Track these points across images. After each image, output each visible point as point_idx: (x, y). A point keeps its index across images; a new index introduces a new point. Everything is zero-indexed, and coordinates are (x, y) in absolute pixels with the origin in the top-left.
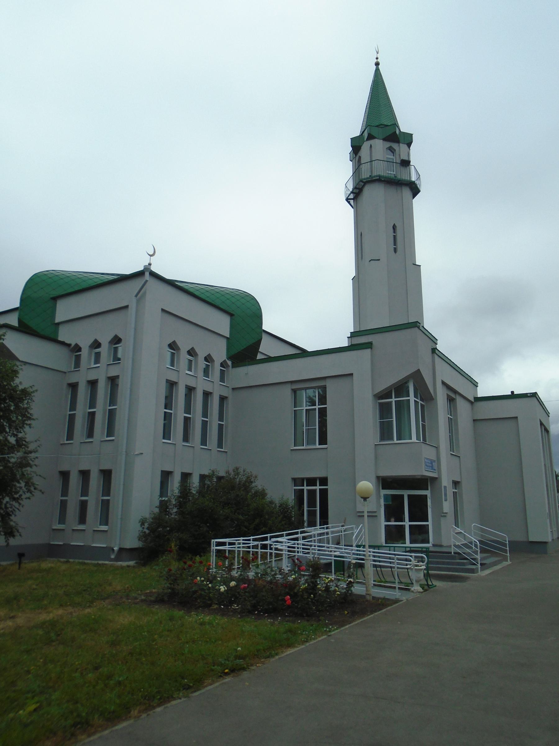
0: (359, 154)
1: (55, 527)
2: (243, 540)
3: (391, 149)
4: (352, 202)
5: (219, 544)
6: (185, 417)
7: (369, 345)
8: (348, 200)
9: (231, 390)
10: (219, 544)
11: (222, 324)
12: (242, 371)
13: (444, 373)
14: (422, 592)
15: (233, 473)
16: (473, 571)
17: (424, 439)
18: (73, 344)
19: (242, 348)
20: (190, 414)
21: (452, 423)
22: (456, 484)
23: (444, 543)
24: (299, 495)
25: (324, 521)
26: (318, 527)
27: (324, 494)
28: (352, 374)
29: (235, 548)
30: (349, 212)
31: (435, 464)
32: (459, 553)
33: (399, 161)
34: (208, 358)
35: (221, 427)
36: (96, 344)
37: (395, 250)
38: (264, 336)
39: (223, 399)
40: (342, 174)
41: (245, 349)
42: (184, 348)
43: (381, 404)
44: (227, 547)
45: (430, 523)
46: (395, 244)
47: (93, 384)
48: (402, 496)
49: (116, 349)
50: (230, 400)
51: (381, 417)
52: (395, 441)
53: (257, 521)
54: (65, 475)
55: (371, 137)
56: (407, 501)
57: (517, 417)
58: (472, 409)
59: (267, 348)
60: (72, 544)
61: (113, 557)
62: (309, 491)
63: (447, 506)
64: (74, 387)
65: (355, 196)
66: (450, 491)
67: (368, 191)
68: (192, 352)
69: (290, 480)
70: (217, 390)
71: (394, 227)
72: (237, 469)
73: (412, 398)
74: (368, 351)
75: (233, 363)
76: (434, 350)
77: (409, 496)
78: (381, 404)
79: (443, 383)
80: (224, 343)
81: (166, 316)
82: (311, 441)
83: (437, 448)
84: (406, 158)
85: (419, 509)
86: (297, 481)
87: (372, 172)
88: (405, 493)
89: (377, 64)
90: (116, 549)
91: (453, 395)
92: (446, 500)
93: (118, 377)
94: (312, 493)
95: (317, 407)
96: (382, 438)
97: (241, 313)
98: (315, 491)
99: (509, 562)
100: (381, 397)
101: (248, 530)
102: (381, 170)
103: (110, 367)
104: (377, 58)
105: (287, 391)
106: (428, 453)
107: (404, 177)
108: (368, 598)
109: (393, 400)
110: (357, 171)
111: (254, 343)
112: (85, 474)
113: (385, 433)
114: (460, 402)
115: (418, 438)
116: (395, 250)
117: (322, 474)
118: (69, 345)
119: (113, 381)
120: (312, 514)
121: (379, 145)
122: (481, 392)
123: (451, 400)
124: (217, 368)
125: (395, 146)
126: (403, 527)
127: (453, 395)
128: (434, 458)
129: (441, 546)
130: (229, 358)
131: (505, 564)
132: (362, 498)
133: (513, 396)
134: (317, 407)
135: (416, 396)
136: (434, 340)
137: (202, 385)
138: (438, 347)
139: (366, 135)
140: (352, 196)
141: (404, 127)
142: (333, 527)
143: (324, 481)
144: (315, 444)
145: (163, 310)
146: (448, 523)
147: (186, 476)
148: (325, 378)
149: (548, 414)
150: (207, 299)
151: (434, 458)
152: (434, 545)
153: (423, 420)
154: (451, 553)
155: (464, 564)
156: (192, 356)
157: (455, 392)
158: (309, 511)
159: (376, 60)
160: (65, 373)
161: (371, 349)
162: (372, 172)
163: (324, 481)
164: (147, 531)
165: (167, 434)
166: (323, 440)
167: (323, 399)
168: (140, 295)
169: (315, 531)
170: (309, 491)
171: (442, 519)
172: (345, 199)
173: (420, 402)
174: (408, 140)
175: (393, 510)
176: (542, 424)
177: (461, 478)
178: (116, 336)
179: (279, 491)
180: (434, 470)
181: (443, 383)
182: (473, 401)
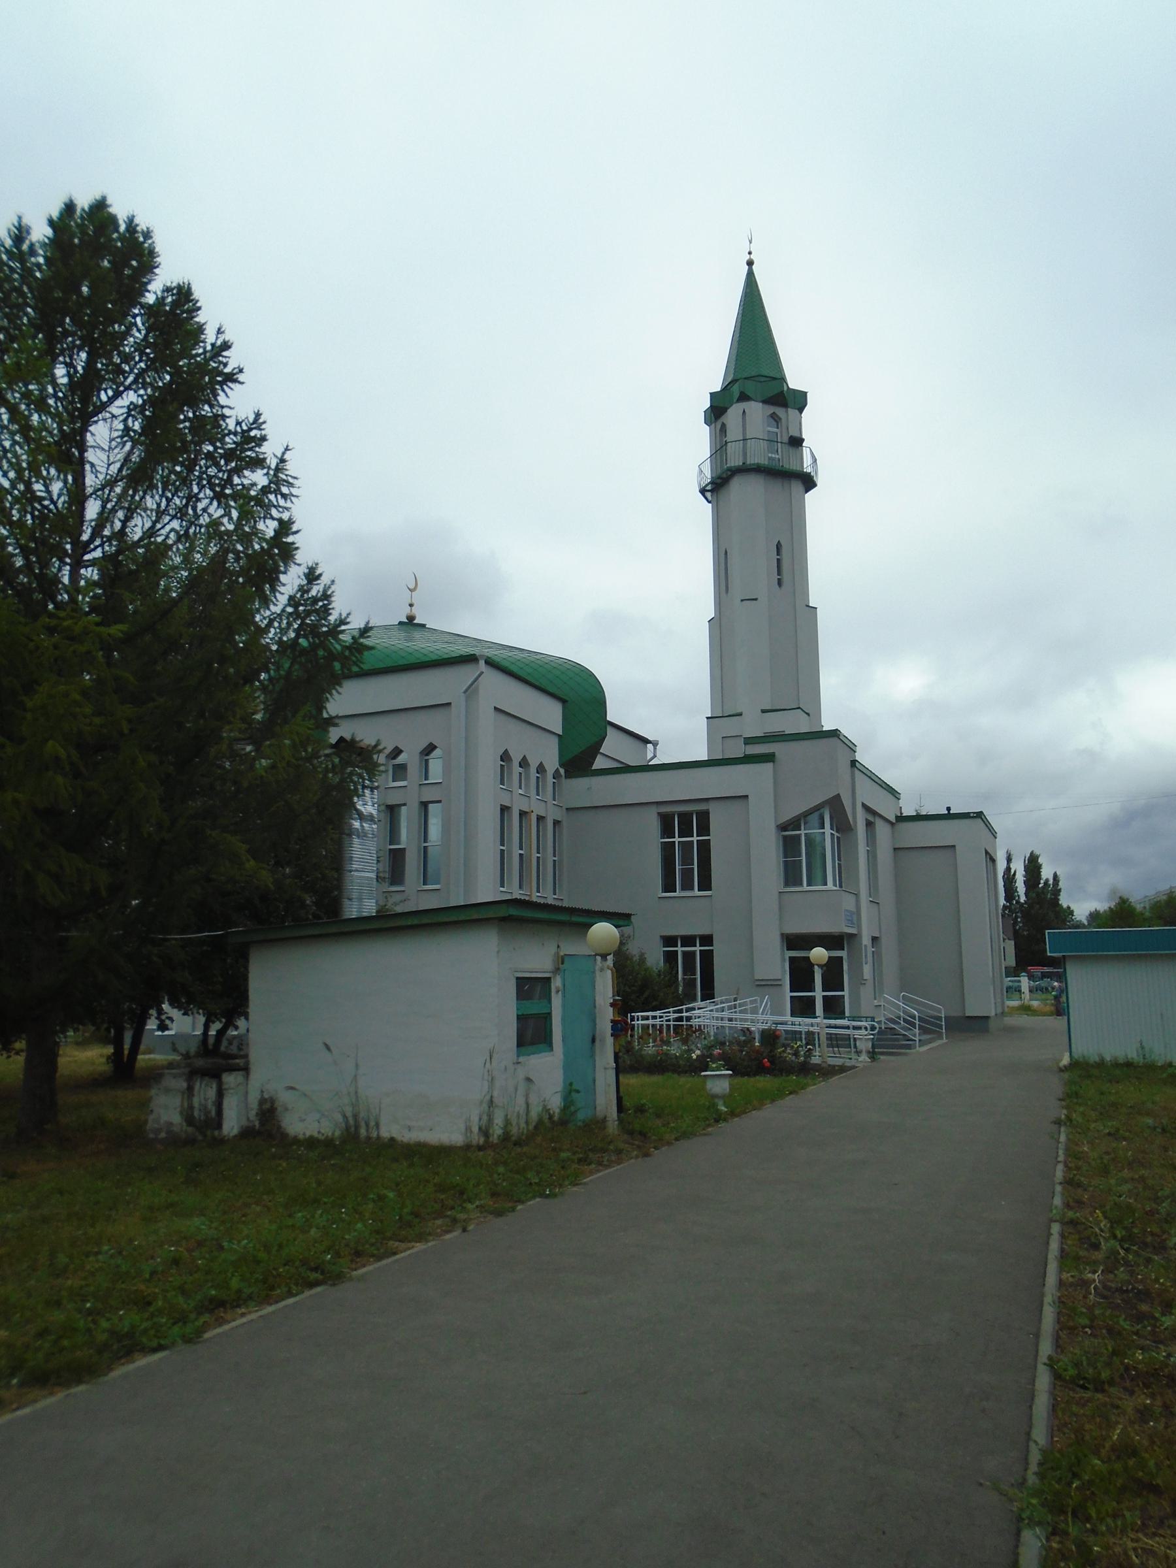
0: (723, 419)
3: (774, 416)
4: (708, 495)
7: (769, 758)
8: (703, 491)
11: (551, 715)
12: (581, 784)
13: (867, 794)
16: (909, 1047)
17: (841, 886)
22: (875, 940)
24: (670, 958)
28: (746, 797)
30: (705, 510)
31: (854, 917)
33: (786, 439)
34: (541, 769)
37: (780, 583)
38: (609, 729)
39: (556, 823)
40: (695, 447)
42: (516, 759)
43: (785, 837)
44: (650, 1022)
45: (846, 993)
46: (779, 573)
49: (427, 761)
50: (564, 824)
52: (805, 887)
55: (743, 397)
57: (954, 846)
62: (684, 953)
63: (867, 971)
65: (716, 487)
66: (870, 950)
67: (739, 487)
68: (524, 763)
69: (658, 939)
70: (552, 814)
71: (779, 547)
73: (828, 830)
74: (769, 766)
76: (854, 763)
78: (785, 837)
79: (864, 805)
80: (556, 740)
81: (503, 717)
82: (687, 886)
83: (857, 895)
84: (796, 434)
85: (833, 975)
86: (669, 941)
87: (745, 454)
89: (750, 263)
91: (871, 818)
94: (689, 957)
95: (695, 839)
96: (787, 883)
97: (575, 695)
99: (945, 1040)
102: (759, 455)
104: (750, 253)
106: (848, 903)
107: (794, 467)
108: (824, 1065)
109: (802, 832)
110: (719, 449)
113: (791, 876)
116: (780, 583)
121: (756, 411)
123: (869, 824)
124: (550, 780)
125: (780, 411)
126: (813, 999)
127: (871, 818)
128: (852, 908)
130: (562, 765)
131: (939, 1042)
133: (949, 816)
134: (695, 839)
136: (851, 748)
137: (538, 809)
138: (858, 757)
139: (736, 389)
140: (709, 488)
141: (794, 381)
143: (707, 940)
144: (692, 889)
145: (496, 708)
146: (866, 992)
148: (707, 800)
149: (994, 834)
150: (521, 673)
151: (852, 908)
153: (839, 859)
155: (897, 1040)
157: (874, 813)
159: (748, 257)
162: (745, 454)
163: (707, 940)
166: (705, 884)
167: (704, 829)
168: (471, 691)
170: (684, 953)
172: (698, 490)
174: (799, 401)
175: (801, 974)
176: (987, 852)
178: (431, 744)
181: (864, 805)
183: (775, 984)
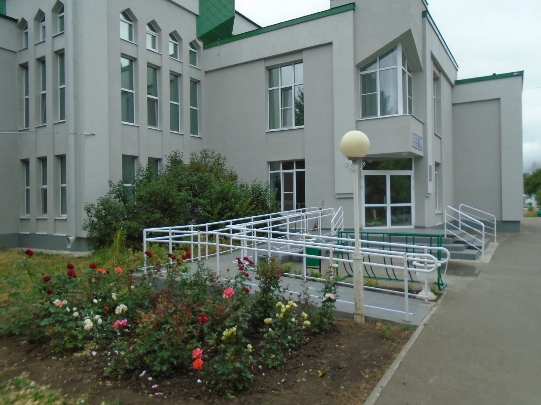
1: (21, 218)
2: (172, 229)
5: (150, 235)
6: (149, 100)
9: (203, 73)
10: (150, 235)
12: (214, 51)
14: (435, 301)
15: (200, 155)
18: (20, 20)
19: (213, 27)
20: (157, 96)
21: (437, 102)
22: (437, 165)
23: (427, 225)
24: (275, 179)
25: (301, 202)
26: (295, 210)
27: (301, 177)
29: (168, 239)
32: (453, 236)
35: (194, 113)
36: (40, 16)
39: (194, 83)
41: (215, 29)
43: (363, 77)
47: (42, 61)
48: (385, 177)
50: (203, 83)
51: (364, 91)
53: (220, 205)
54: (26, 162)
56: (387, 183)
57: (499, 99)
58: (452, 93)
59: (239, 28)
60: (37, 233)
61: (69, 247)
62: (285, 175)
63: (431, 187)
64: (25, 67)
66: (434, 172)
68: (153, 26)
69: (266, 163)
70: (188, 73)
72: (205, 151)
74: (350, 14)
75: (204, 44)
76: (425, 13)
77: (392, 177)
78: (363, 77)
80: (192, 21)
85: (402, 190)
86: (272, 165)
88: (388, 174)
90: (72, 238)
91: (438, 73)
92: (430, 181)
93: (63, 49)
94: (288, 177)
96: (364, 115)
98: (291, 174)
100: (363, 69)
101: (212, 215)
103: (56, 39)
105: (261, 68)
106: (416, 128)
108: (359, 320)
111: (226, 22)
112: (43, 160)
114: (444, 83)
115: (404, 111)
117: (298, 157)
118: (15, 21)
119: (60, 54)
120: (288, 197)
122: (461, 76)
123: (436, 79)
124: (186, 48)
127: (438, 73)
128: (420, 134)
129: (423, 228)
132: (350, 158)
133: (495, 77)
135: (403, 65)
142: (309, 210)
143: (301, 164)
147: (154, 162)
148: (300, 51)
152: (416, 227)
153: (410, 94)
154: (443, 236)
155: (460, 249)
156: (156, 32)
157: (441, 70)
158: (285, 195)
160: (16, 52)
161: (354, 10)
163: (301, 164)
164: (95, 220)
165: (128, 114)
169: (287, 215)
171: (426, 200)
173: (407, 73)
175: (374, 190)
177: (441, 160)
179: (252, 172)
180: (421, 148)
182: (453, 83)
183: (348, 197)
